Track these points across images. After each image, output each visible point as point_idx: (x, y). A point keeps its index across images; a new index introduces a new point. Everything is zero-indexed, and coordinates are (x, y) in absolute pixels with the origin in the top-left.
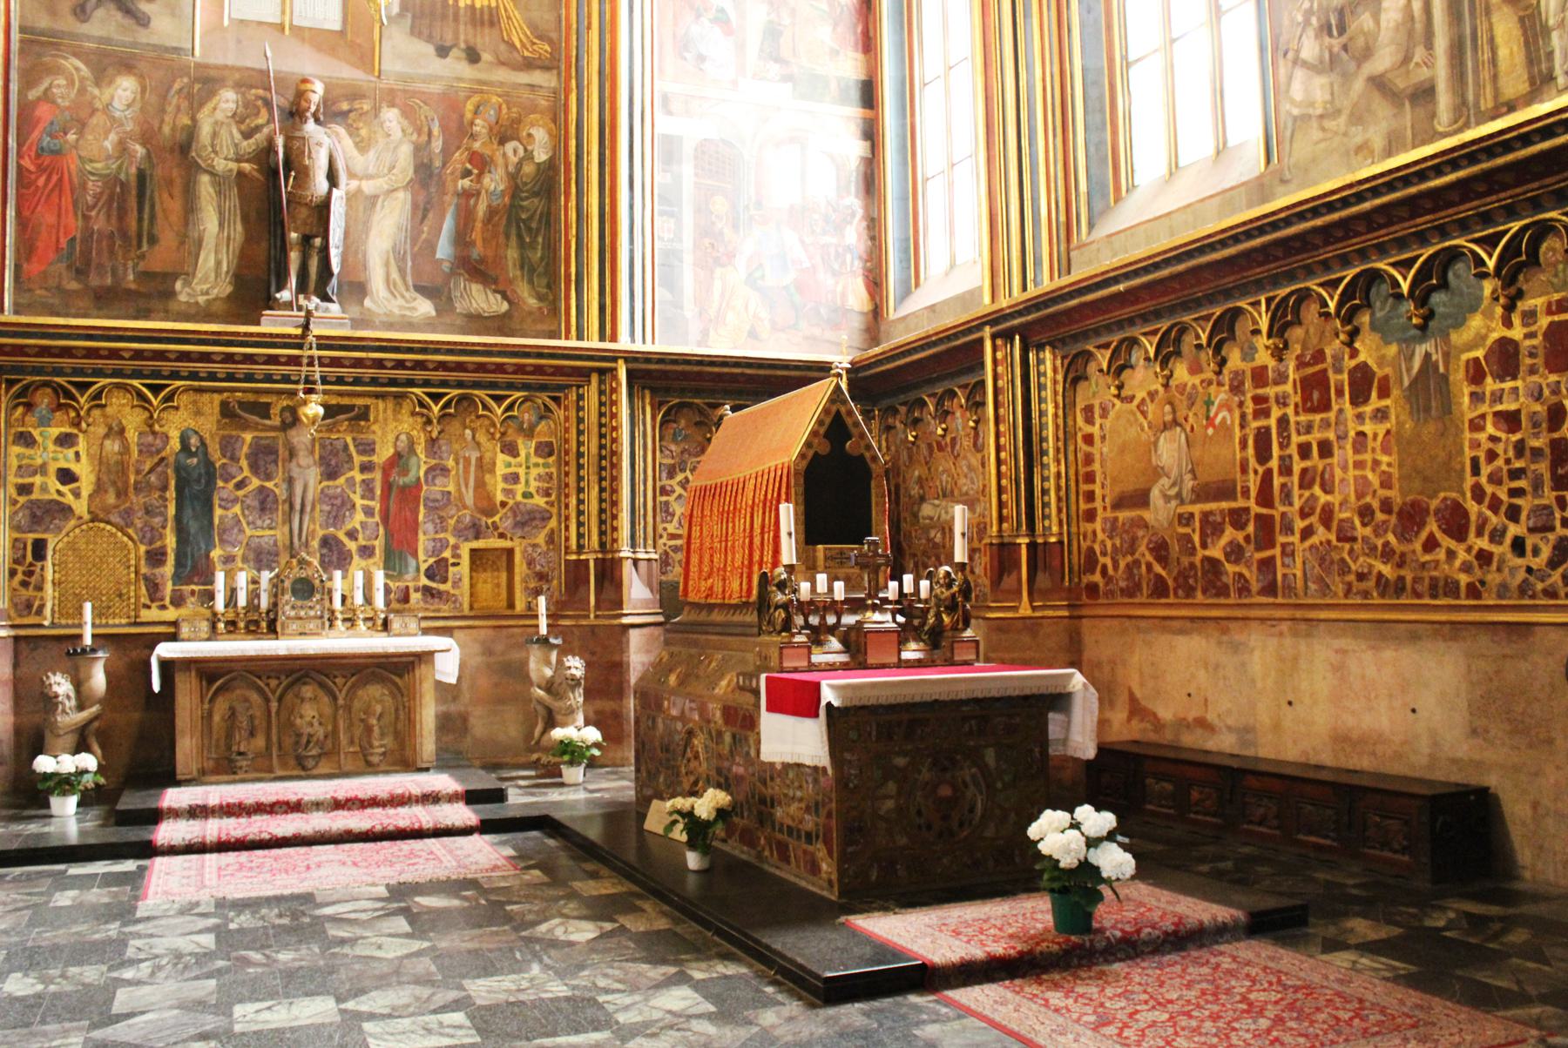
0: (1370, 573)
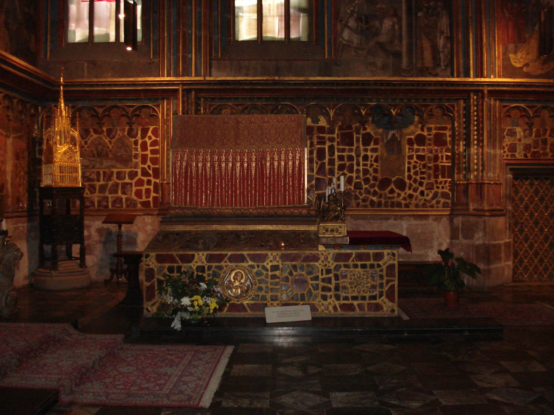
0: (368, 200)
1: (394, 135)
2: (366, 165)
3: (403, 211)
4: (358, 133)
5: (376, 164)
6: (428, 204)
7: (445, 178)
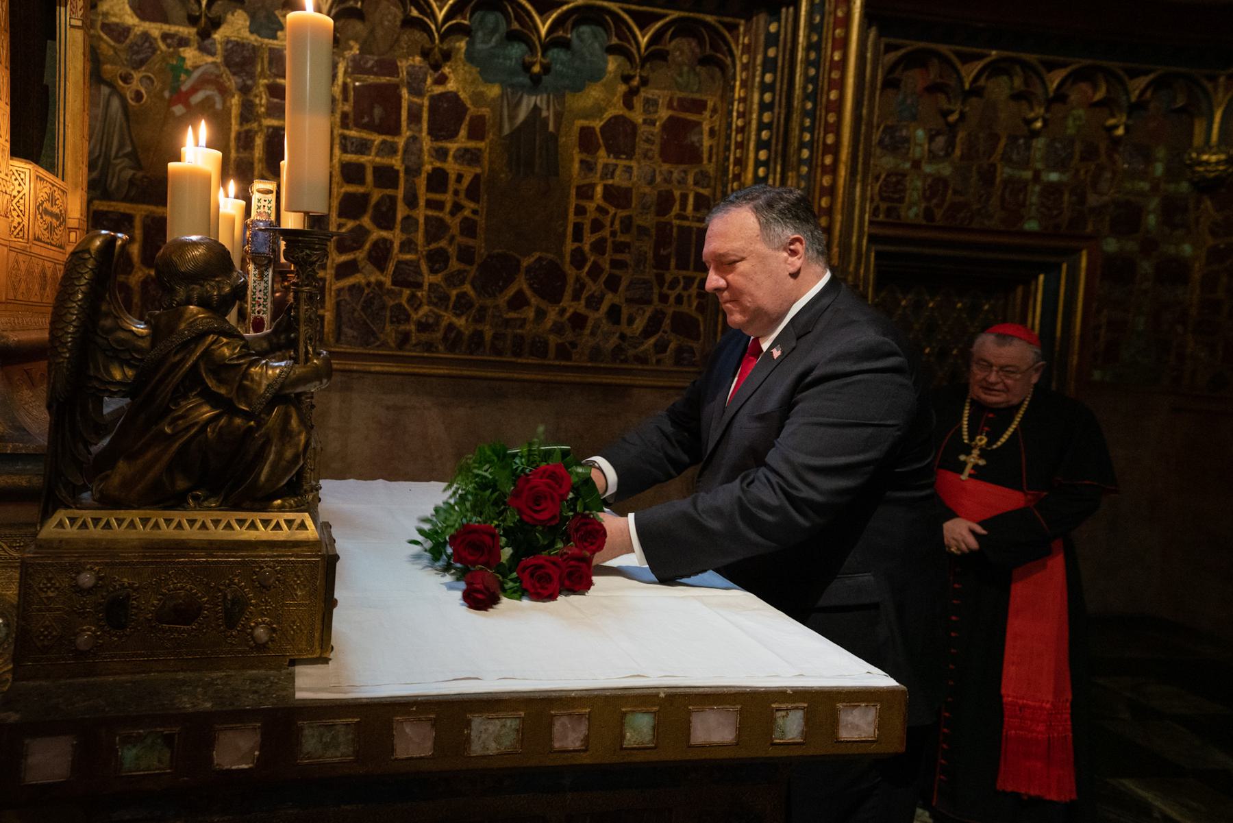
0: (437, 323)
1: (536, 110)
2: (439, 206)
3: (549, 368)
4: (416, 91)
5: (472, 205)
6: (631, 352)
7: (686, 268)
